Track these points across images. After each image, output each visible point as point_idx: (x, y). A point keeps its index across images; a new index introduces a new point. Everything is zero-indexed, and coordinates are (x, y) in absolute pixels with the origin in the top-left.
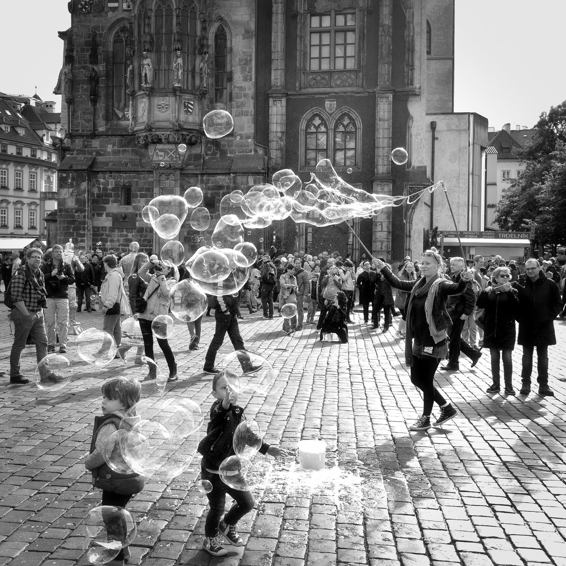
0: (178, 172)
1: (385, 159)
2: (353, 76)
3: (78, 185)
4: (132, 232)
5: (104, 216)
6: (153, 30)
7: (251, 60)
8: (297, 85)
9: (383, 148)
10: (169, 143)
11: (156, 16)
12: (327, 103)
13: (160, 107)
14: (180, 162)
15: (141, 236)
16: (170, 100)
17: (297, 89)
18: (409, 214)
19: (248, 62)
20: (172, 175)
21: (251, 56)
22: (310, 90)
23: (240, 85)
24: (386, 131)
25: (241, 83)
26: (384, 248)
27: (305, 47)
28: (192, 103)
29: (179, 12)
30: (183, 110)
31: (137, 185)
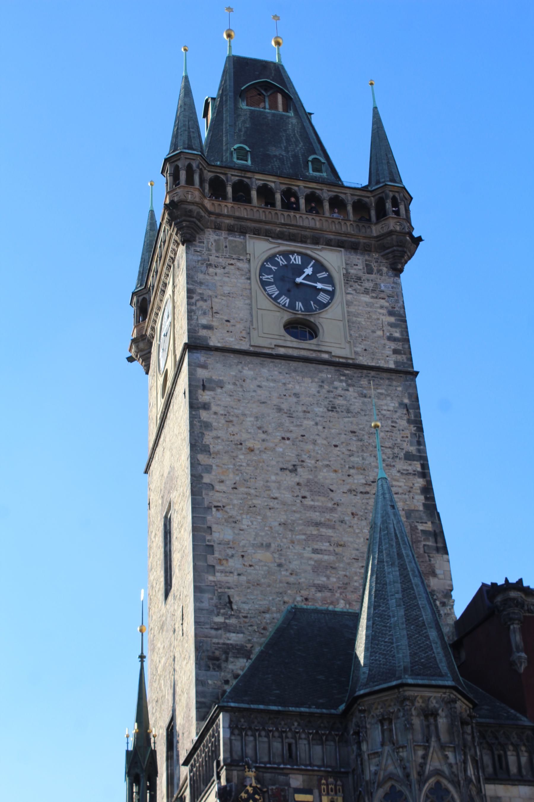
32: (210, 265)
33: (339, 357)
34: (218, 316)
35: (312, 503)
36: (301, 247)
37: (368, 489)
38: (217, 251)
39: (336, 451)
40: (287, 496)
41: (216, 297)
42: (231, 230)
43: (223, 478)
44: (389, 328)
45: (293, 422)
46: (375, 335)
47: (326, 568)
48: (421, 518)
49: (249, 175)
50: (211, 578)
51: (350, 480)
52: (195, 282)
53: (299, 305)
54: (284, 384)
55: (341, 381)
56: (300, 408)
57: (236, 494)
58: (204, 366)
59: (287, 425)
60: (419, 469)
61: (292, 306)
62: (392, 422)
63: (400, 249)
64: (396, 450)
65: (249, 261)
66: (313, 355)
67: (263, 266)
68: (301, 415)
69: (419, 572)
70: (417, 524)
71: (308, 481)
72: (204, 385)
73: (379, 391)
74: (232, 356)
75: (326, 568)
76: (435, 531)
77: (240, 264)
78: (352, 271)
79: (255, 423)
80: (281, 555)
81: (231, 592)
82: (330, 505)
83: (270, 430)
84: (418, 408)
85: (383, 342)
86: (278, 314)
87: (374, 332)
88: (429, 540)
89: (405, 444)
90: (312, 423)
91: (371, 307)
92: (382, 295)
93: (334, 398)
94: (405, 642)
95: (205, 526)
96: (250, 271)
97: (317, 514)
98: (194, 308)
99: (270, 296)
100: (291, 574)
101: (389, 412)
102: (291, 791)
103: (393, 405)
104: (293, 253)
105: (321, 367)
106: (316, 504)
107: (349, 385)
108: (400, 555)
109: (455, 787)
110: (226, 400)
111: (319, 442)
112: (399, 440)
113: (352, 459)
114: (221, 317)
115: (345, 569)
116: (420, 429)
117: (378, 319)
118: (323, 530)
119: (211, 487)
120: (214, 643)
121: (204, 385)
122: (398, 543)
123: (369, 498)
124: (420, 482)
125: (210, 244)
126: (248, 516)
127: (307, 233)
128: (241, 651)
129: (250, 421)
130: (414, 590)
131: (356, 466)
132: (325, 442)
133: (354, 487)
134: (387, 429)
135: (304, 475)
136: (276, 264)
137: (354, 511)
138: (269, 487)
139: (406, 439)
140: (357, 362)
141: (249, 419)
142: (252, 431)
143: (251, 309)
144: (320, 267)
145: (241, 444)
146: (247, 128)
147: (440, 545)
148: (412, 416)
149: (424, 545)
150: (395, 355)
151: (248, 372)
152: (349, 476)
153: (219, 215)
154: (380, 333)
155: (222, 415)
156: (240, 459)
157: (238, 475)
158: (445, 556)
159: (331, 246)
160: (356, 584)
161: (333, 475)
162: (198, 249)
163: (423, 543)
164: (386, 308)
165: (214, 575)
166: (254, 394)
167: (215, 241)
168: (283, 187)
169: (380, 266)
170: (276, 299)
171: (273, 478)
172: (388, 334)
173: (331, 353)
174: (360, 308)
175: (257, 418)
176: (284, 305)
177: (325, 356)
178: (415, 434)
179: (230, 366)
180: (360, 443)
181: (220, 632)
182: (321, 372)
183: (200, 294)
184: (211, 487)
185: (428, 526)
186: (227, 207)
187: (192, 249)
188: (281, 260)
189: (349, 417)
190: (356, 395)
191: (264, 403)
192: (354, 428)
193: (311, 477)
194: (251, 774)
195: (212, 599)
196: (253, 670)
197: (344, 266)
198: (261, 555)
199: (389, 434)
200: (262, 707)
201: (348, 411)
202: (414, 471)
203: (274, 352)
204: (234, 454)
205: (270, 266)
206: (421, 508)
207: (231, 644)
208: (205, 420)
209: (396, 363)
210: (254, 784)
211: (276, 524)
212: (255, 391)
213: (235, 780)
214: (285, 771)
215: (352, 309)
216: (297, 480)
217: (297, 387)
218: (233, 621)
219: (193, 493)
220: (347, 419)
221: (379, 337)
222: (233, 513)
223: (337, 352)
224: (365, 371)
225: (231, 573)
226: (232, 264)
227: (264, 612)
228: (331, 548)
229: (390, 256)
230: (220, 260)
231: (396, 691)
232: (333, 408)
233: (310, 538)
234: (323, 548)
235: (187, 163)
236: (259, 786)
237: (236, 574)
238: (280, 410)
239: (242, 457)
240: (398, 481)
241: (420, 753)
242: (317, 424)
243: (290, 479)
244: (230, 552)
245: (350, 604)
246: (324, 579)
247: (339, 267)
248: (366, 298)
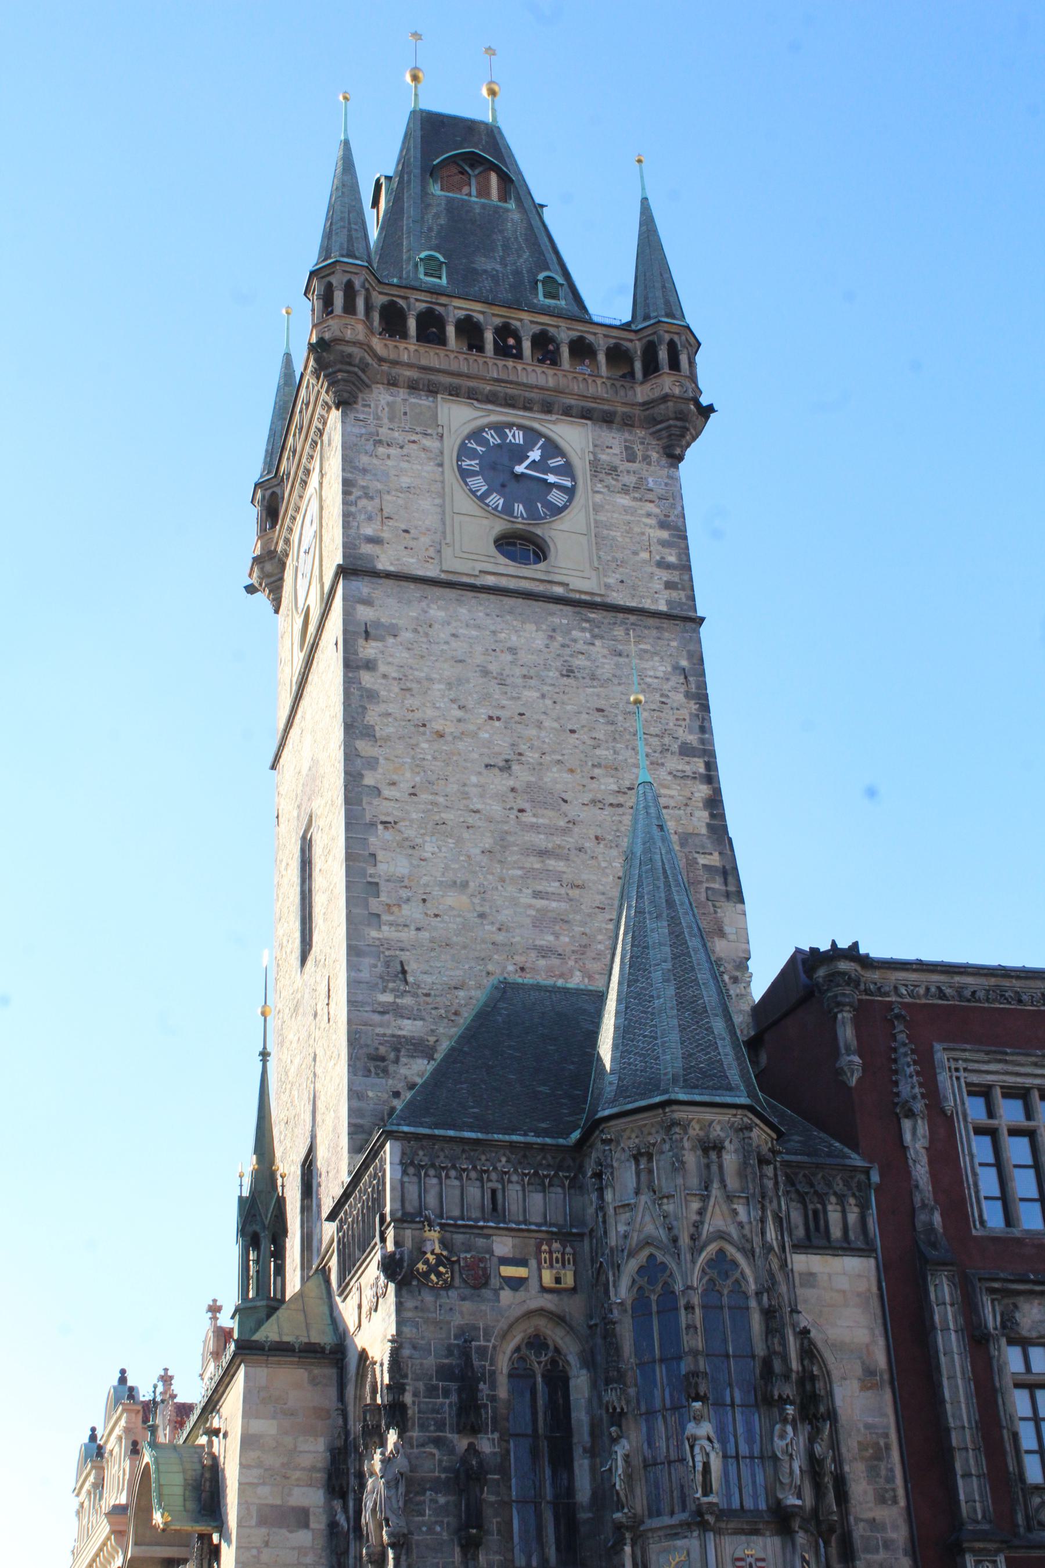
7: (888, 1447)
8: (1020, 1519)
17: (1022, 1530)
21: (886, 1435)
23: (869, 1515)
25: (870, 1509)
32: (380, 442)
33: (581, 592)
34: (391, 523)
35: (534, 820)
36: (523, 417)
37: (621, 799)
38: (391, 419)
39: (572, 739)
40: (496, 809)
41: (388, 492)
42: (413, 387)
43: (395, 777)
44: (660, 547)
45: (506, 693)
46: (637, 558)
47: (554, 921)
48: (703, 847)
49: (443, 300)
50: (374, 934)
51: (594, 785)
52: (356, 468)
53: (519, 508)
54: (494, 632)
55: (583, 630)
56: (518, 671)
57: (416, 803)
58: (368, 602)
59: (496, 697)
60: (702, 770)
61: (508, 510)
62: (662, 695)
63: (678, 423)
64: (667, 740)
65: (442, 436)
66: (540, 588)
67: (463, 447)
68: (519, 681)
69: (699, 929)
70: (696, 855)
71: (529, 785)
72: (366, 632)
73: (642, 646)
74: (412, 586)
75: (554, 921)
76: (724, 867)
77: (427, 442)
78: (603, 457)
79: (447, 693)
80: (484, 900)
81: (405, 956)
82: (562, 823)
83: (470, 704)
84: (703, 674)
85: (649, 569)
86: (485, 522)
87: (635, 553)
88: (714, 881)
89: (681, 730)
90: (537, 694)
91: (632, 515)
92: (650, 496)
93: (571, 656)
94: (675, 1036)
95: (367, 853)
96: (442, 453)
97: (542, 836)
98: (353, 509)
99: (474, 493)
100: (500, 930)
101: (656, 681)
102: (495, 1260)
103: (664, 669)
104: (510, 426)
105: (552, 607)
106: (541, 821)
107: (594, 636)
108: (670, 903)
109: (747, 1257)
110: (402, 656)
111: (546, 724)
112: (671, 724)
113: (598, 752)
114: (396, 524)
116: (705, 708)
117: (643, 534)
118: (552, 863)
119: (377, 791)
120: (378, 1035)
121: (366, 632)
122: (667, 885)
123: (623, 814)
124: (703, 791)
125: (380, 408)
126: (434, 839)
127: (533, 395)
128: (421, 1048)
129: (439, 690)
130: (690, 957)
131: (603, 763)
132: (556, 725)
133: (599, 797)
134: (653, 707)
135: (521, 775)
136: (484, 442)
137: (599, 834)
138: (467, 794)
139: (683, 723)
140: (609, 600)
141: (437, 686)
142: (442, 705)
143: (444, 513)
144: (552, 448)
145: (424, 725)
146: (441, 225)
147: (732, 888)
148: (693, 686)
149: (707, 888)
150: (668, 592)
151: (436, 613)
152: (592, 778)
153: (395, 363)
154: (645, 555)
155: (395, 679)
156: (423, 749)
157: (418, 773)
158: (739, 906)
159: (571, 416)
160: (600, 947)
162: (361, 417)
163: (705, 885)
164: (656, 516)
165: (379, 928)
166: (445, 647)
167: (388, 404)
168: (498, 321)
169: (647, 450)
170: (482, 498)
171: (474, 779)
172: (658, 558)
173: (568, 585)
174: (615, 515)
175: (450, 685)
176: (496, 509)
177: (559, 590)
178: (697, 716)
179: (409, 602)
180: (611, 728)
181: (387, 1017)
182: (552, 614)
183: (363, 487)
184: (377, 791)
186: (409, 350)
187: (352, 416)
188: (492, 436)
189: (594, 687)
190: (605, 651)
191: (460, 661)
192: (602, 703)
193: (533, 779)
194: (433, 1235)
195: (376, 966)
196: (438, 1078)
197: (591, 449)
198: (453, 899)
199: (656, 714)
200: (451, 1133)
201: (593, 677)
202: (694, 773)
203: (478, 582)
204: (413, 741)
205: (475, 446)
206: (704, 831)
207: (404, 1037)
208: (368, 686)
209: (669, 603)
210: (437, 1251)
211: (478, 851)
212: (447, 643)
213: (408, 1244)
214: (486, 1231)
216: (511, 783)
217: (514, 638)
218: (407, 1001)
219: (348, 801)
220: (592, 690)
221: (644, 561)
222: (410, 833)
223: (577, 583)
224: (621, 615)
225: (405, 926)
226: (414, 442)
227: (456, 988)
228: (563, 891)
229: (664, 434)
230: (396, 434)
231: (660, 1111)
232: (569, 673)
233: (530, 874)
234: (550, 890)
235: (345, 279)
236: (445, 1253)
237: (413, 928)
238: (485, 673)
239: (425, 745)
240: (668, 788)
241: (695, 1205)
242: (543, 696)
243: (499, 782)
244: (404, 893)
245: (590, 977)
246: (551, 938)
247: (582, 450)
248: (624, 501)
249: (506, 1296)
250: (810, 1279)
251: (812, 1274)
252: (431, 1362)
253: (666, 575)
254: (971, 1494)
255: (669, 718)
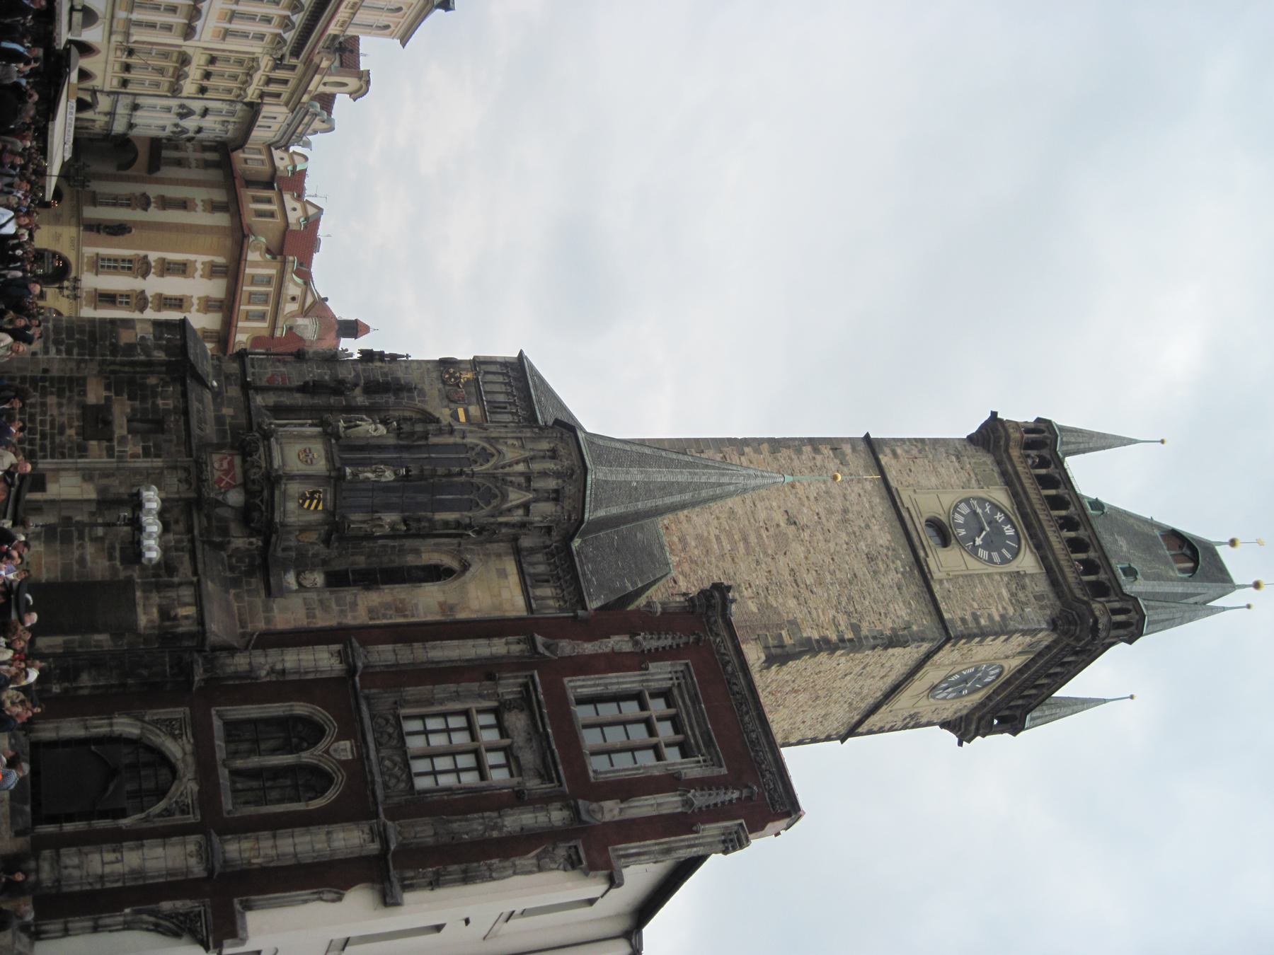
0: (193, 495)
1: (253, 854)
2: (402, 785)
3: (159, 347)
4: (77, 434)
5: (105, 394)
6: (433, 440)
7: (405, 616)
9: (275, 847)
10: (245, 473)
11: (455, 445)
12: (346, 744)
13: (307, 452)
14: (212, 495)
15: (70, 448)
16: (320, 466)
17: (367, 691)
18: (145, 917)
19: (400, 611)
20: (186, 487)
21: (413, 616)
22: (364, 708)
23: (360, 602)
24: (309, 847)
26: (66, 872)
27: (442, 702)
28: (320, 508)
29: (467, 475)
30: (307, 489)
31: (166, 441)
32: (958, 458)
39: (828, 560)
42: (1004, 474)
51: (804, 571)
55: (903, 567)
56: (856, 529)
58: (854, 449)
66: (917, 543)
78: (1027, 581)
87: (973, 600)
99: (957, 506)
115: (710, 563)
118: (741, 545)
122: (719, 468)
124: (834, 637)
140: (932, 583)
144: (1016, 554)
154: (976, 605)
161: (802, 556)
168: (1077, 518)
175: (827, 492)
177: (922, 554)
185: (788, 641)
192: (860, 574)
194: (469, 375)
206: (805, 635)
209: (952, 620)
213: (462, 366)
215: (986, 580)
216: (782, 524)
219: (729, 440)
221: (971, 606)
232: (870, 558)
238: (845, 511)
249: (447, 411)
250: (503, 574)
251: (506, 576)
252: (400, 374)
253: (968, 617)
254: (384, 654)
255: (874, 617)
